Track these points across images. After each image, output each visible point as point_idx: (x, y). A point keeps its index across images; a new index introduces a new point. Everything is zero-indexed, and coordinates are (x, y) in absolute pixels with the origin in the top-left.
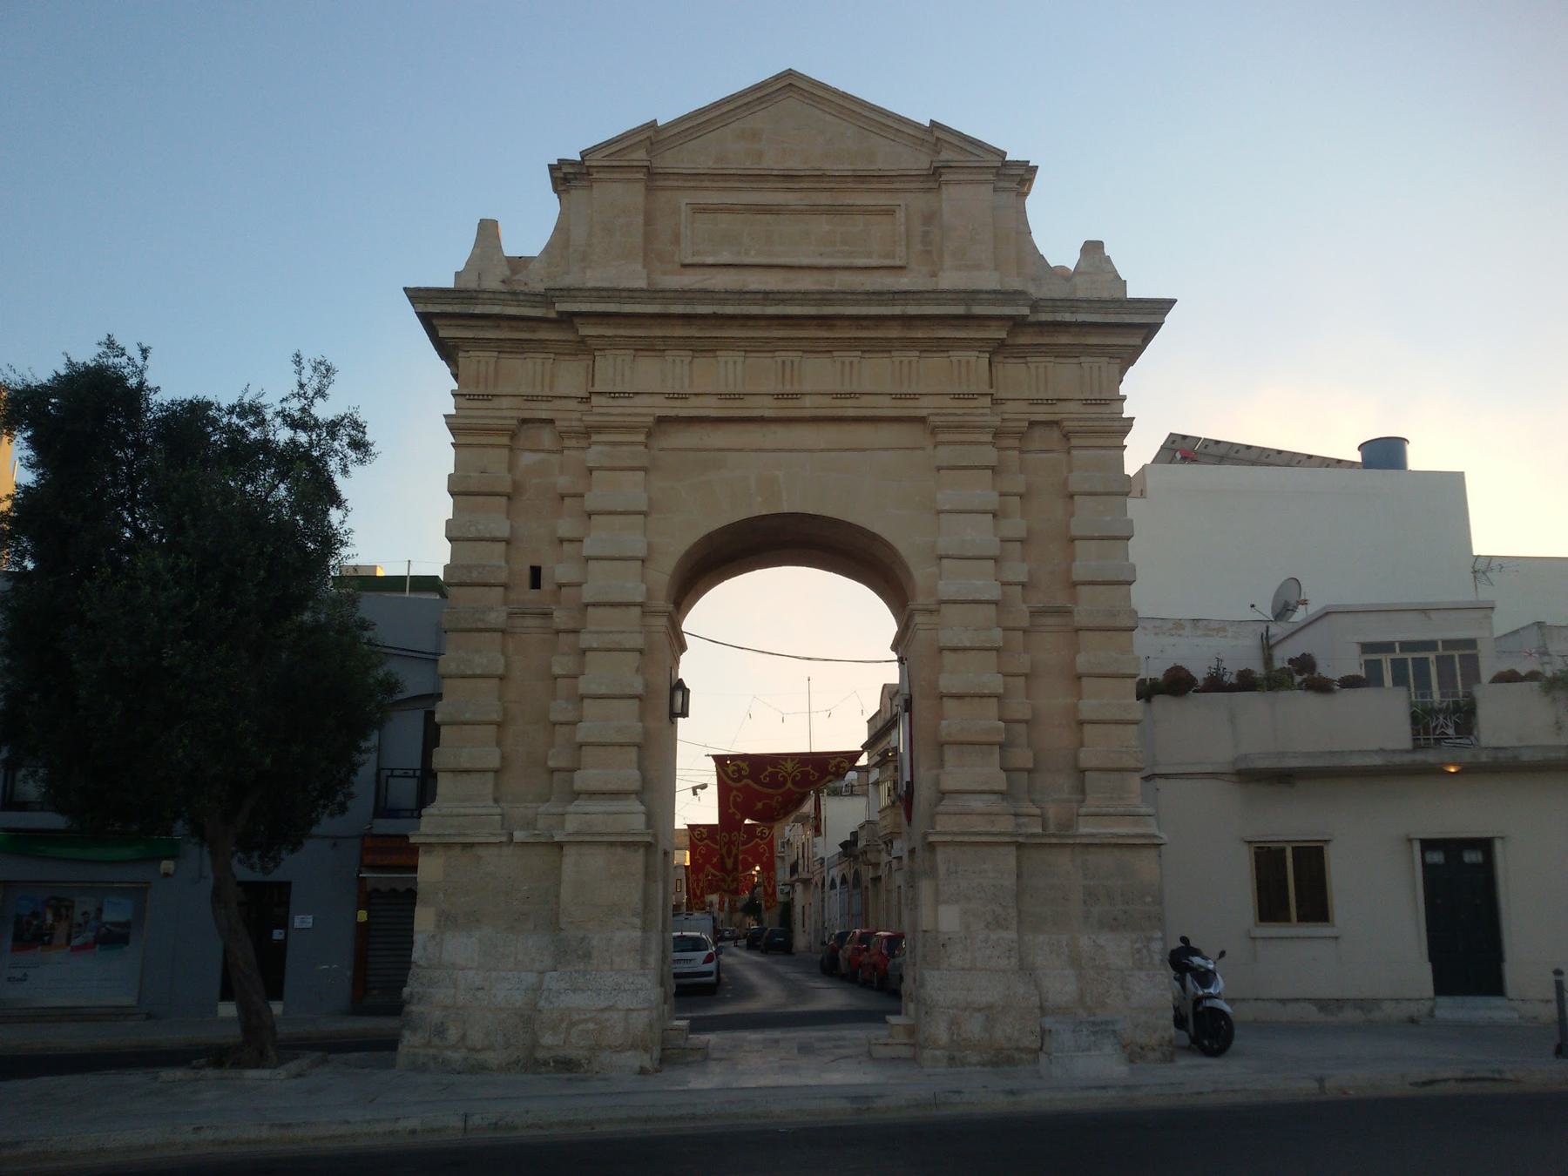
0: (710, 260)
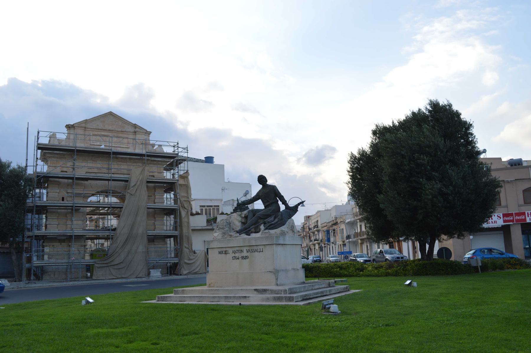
0: (95, 144)
